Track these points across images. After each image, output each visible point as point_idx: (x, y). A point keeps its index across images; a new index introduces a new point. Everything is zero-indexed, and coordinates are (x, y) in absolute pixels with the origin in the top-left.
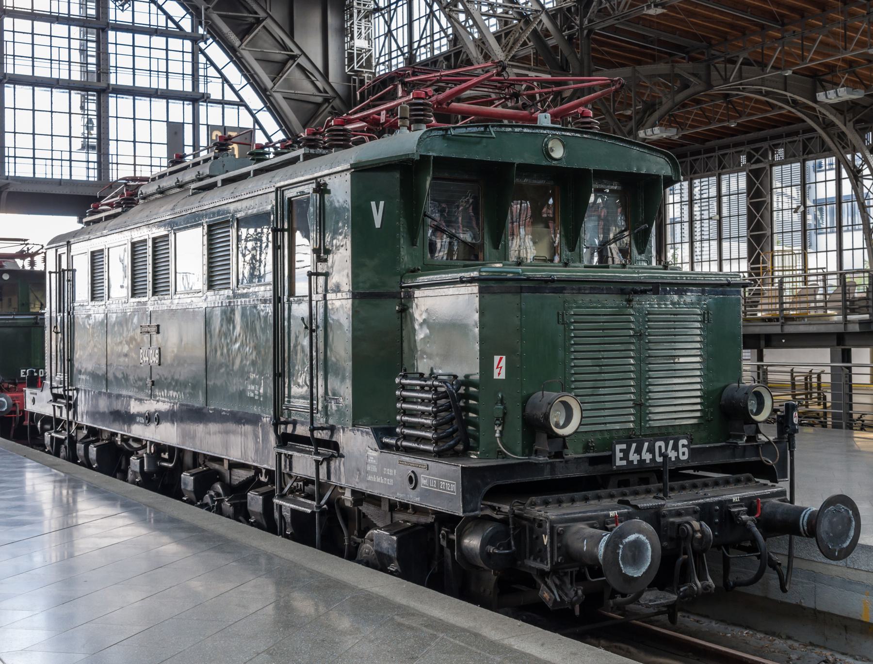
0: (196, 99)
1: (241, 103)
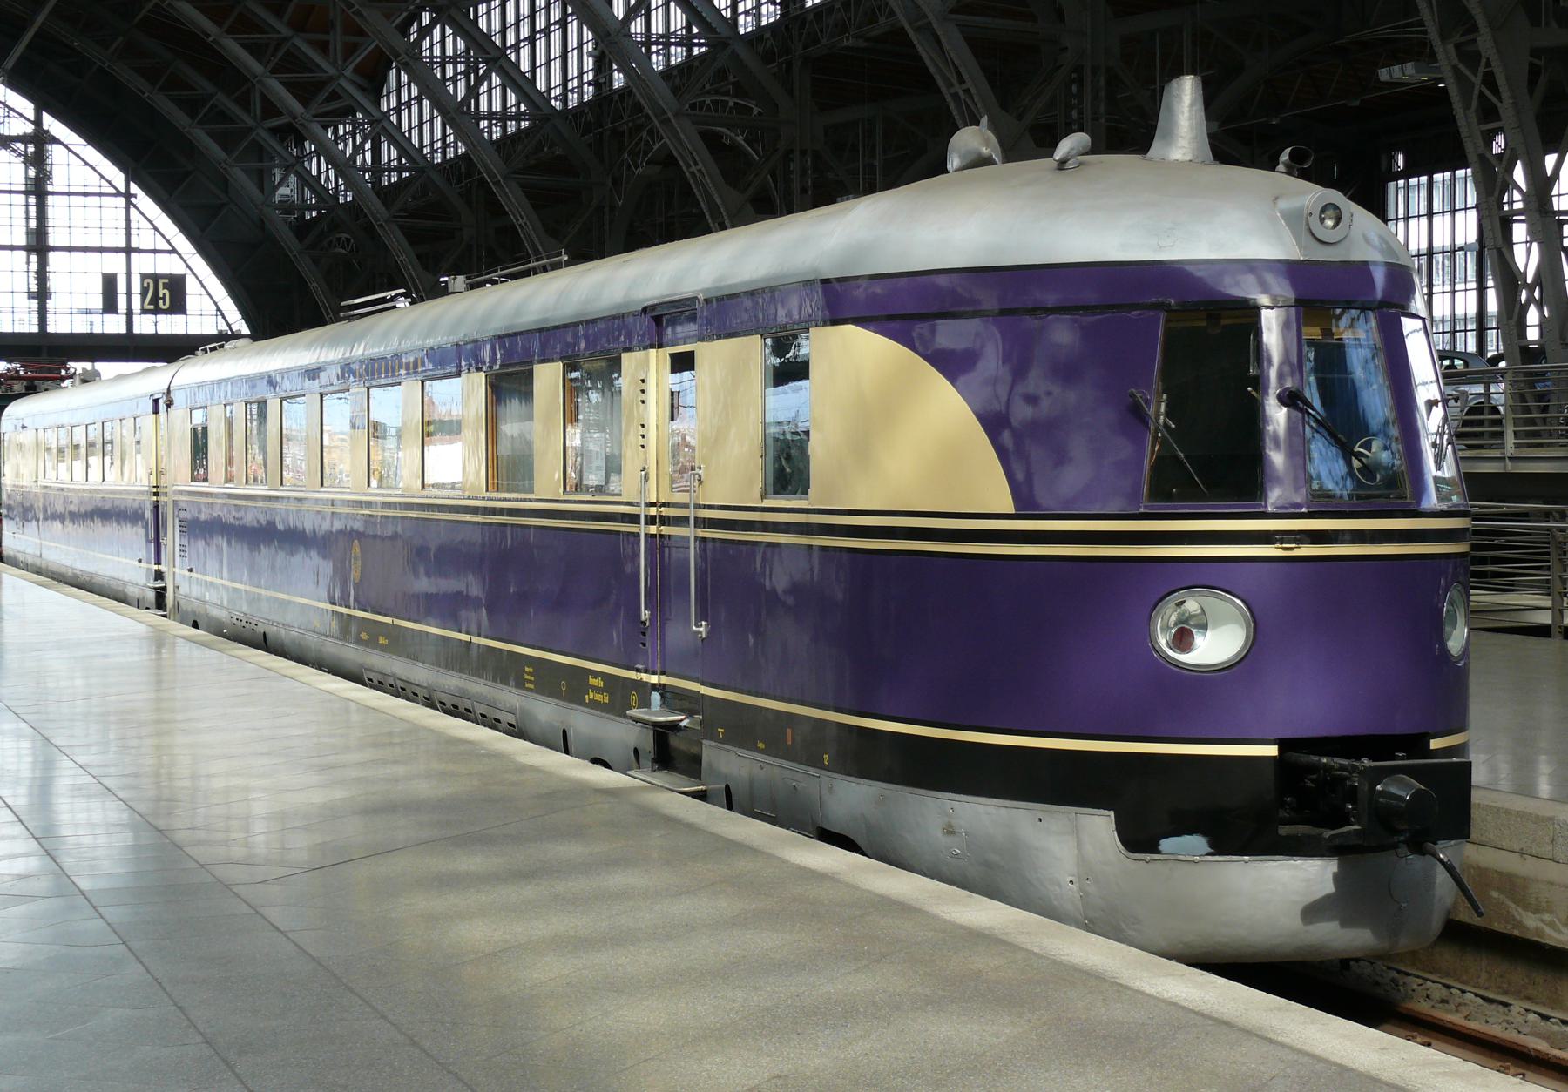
0: (128, 250)
1: (174, 251)
